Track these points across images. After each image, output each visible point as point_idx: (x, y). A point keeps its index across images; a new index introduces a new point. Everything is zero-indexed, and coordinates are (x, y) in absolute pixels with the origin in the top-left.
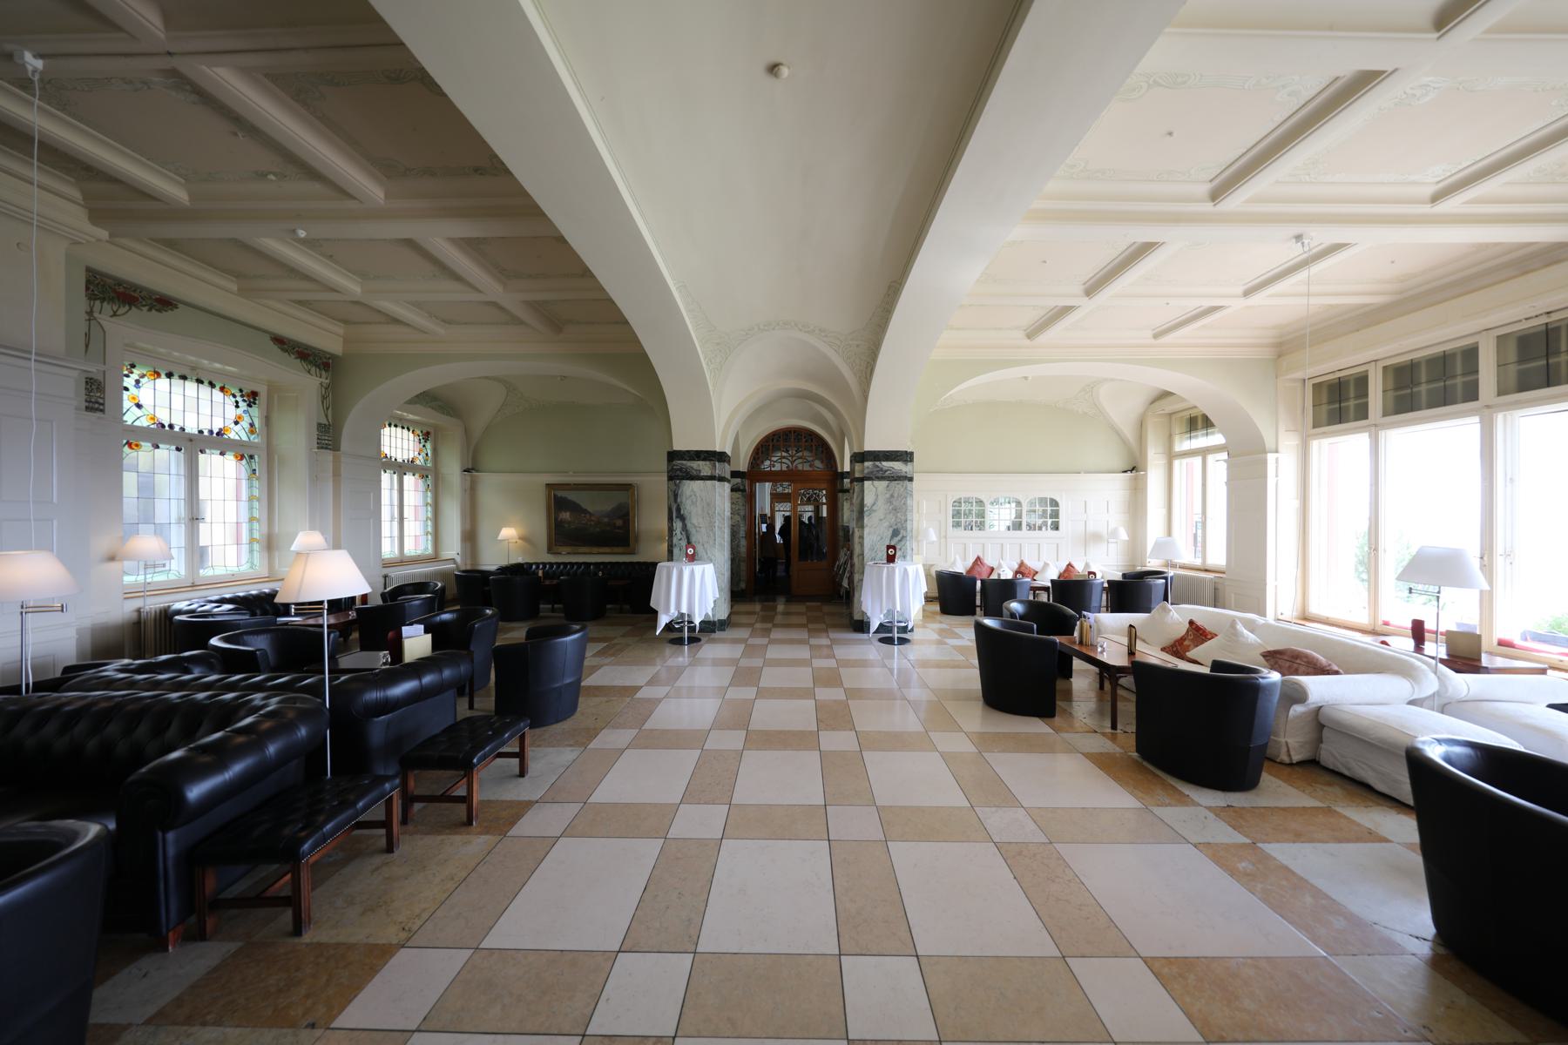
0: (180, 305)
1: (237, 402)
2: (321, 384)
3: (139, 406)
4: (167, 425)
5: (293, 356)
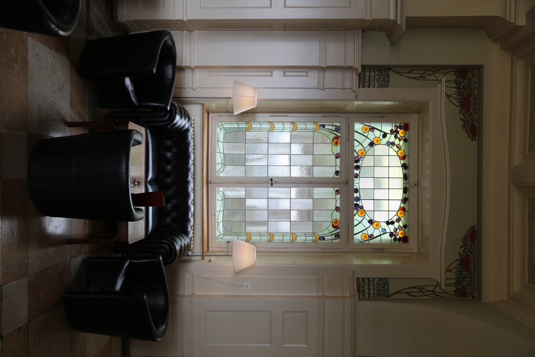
0: (475, 143)
1: (392, 223)
2: (439, 285)
3: (372, 144)
4: (358, 164)
5: (461, 251)
